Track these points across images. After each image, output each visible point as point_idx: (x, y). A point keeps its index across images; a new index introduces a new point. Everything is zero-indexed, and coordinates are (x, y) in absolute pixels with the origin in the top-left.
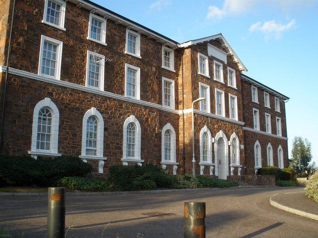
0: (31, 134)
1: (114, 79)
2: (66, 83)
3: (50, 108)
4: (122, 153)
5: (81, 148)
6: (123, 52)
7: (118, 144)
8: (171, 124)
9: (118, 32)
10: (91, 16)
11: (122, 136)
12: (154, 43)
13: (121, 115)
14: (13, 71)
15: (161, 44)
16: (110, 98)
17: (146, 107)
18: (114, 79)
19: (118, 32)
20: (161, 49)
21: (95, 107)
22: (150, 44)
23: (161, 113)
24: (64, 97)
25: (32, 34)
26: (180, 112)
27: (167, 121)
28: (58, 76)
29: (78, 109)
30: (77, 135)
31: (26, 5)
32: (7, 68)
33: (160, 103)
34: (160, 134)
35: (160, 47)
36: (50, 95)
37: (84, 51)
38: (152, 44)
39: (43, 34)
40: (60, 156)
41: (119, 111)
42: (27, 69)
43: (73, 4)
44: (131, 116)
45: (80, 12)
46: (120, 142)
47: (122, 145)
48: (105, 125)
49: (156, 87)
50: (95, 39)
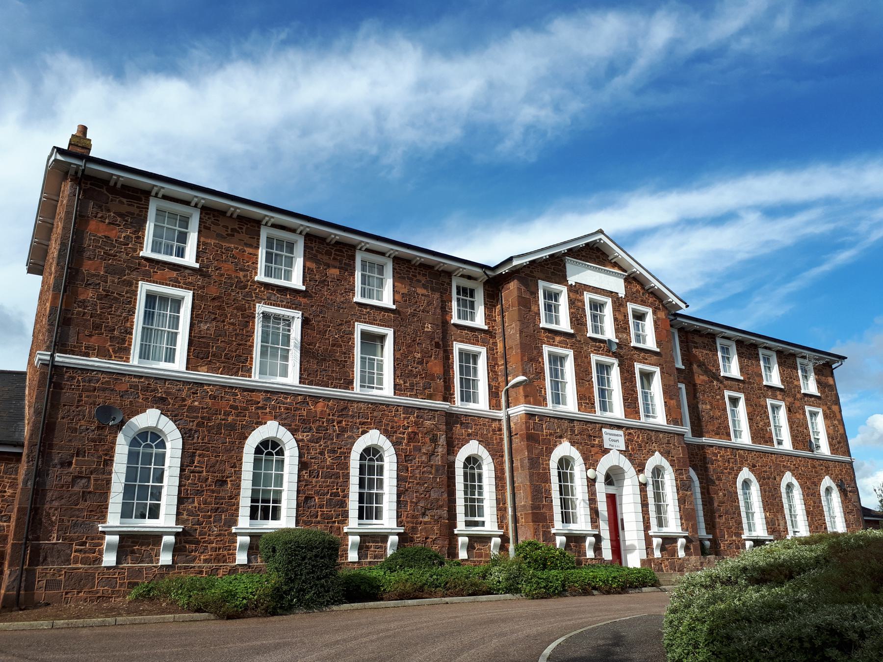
0: (109, 488)
1: (221, 340)
2: (202, 375)
3: (161, 431)
4: (345, 515)
5: (237, 510)
6: (349, 301)
7: (336, 494)
8: (480, 442)
9: (334, 259)
10: (153, 207)
11: (347, 476)
12: (428, 275)
13: (343, 430)
14: (59, 358)
15: (254, 224)
16: (316, 398)
17: (409, 409)
18: (325, 357)
19: (334, 259)
20: (450, 285)
21: (275, 418)
22: (419, 277)
23: (452, 419)
24: (196, 403)
25: (116, 280)
26: (501, 414)
27: (469, 435)
28: (179, 365)
29: (232, 427)
30: (225, 481)
31: (101, 224)
32: (52, 356)
33: (448, 396)
34: (451, 466)
35: (447, 280)
36: (161, 403)
37: (247, 305)
38: (424, 275)
39: (143, 280)
40: (181, 530)
41: (339, 422)
42: (103, 353)
43: (218, 211)
44: (269, 422)
45: (236, 227)
46: (343, 491)
47: (346, 496)
48: (301, 456)
49: (435, 367)
50: (159, 252)
